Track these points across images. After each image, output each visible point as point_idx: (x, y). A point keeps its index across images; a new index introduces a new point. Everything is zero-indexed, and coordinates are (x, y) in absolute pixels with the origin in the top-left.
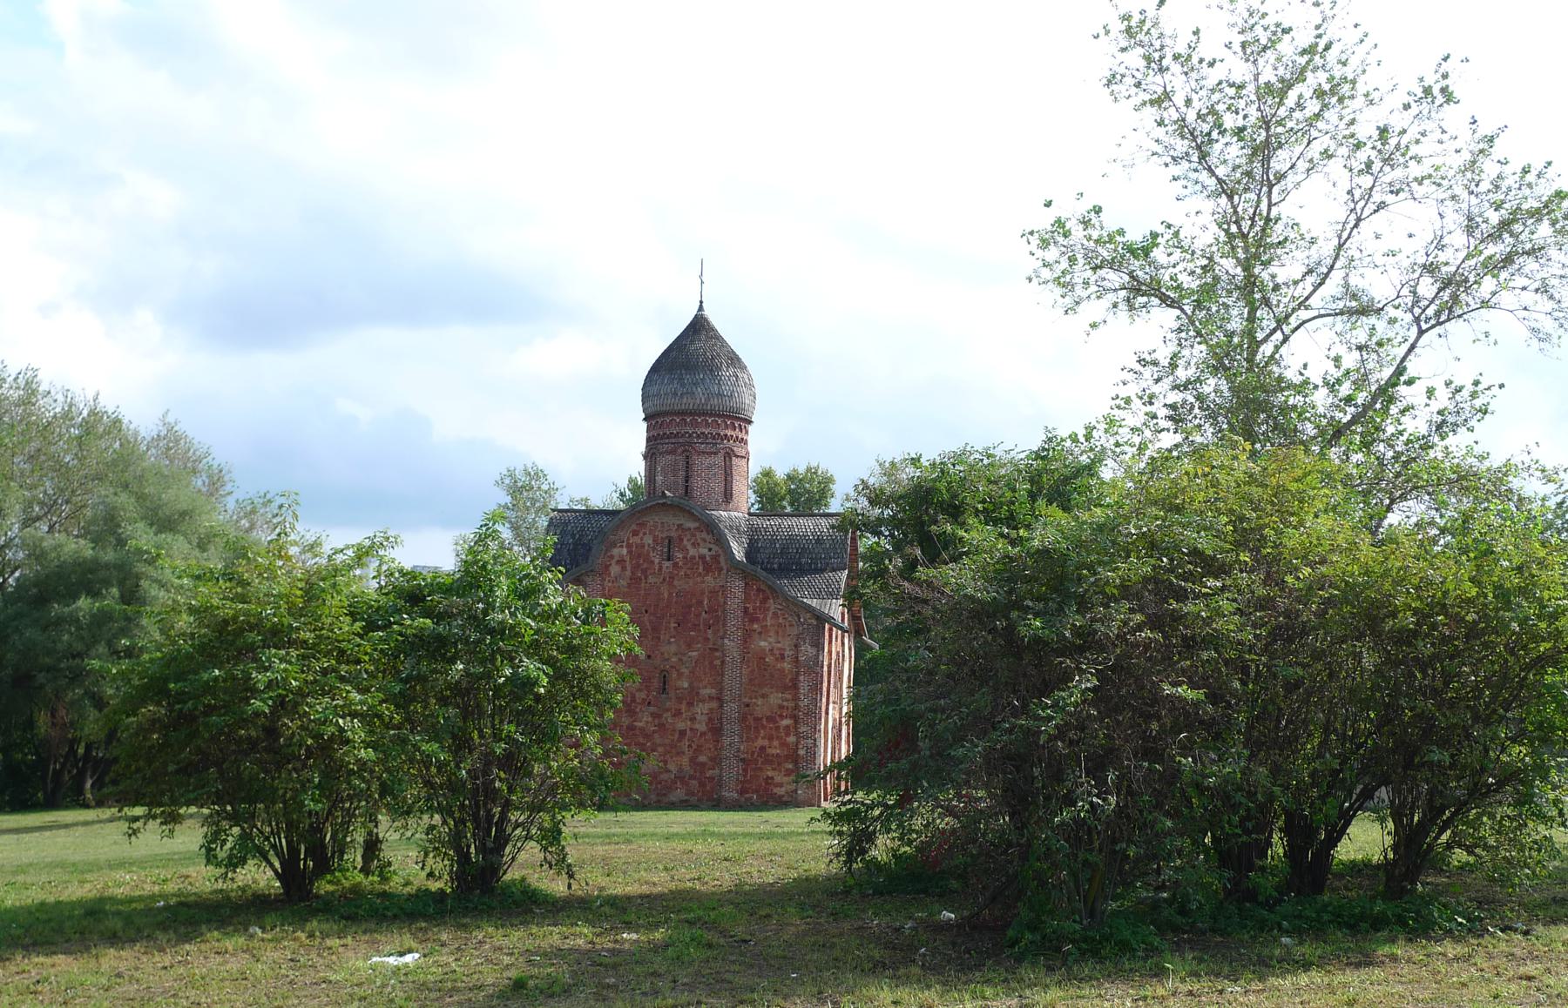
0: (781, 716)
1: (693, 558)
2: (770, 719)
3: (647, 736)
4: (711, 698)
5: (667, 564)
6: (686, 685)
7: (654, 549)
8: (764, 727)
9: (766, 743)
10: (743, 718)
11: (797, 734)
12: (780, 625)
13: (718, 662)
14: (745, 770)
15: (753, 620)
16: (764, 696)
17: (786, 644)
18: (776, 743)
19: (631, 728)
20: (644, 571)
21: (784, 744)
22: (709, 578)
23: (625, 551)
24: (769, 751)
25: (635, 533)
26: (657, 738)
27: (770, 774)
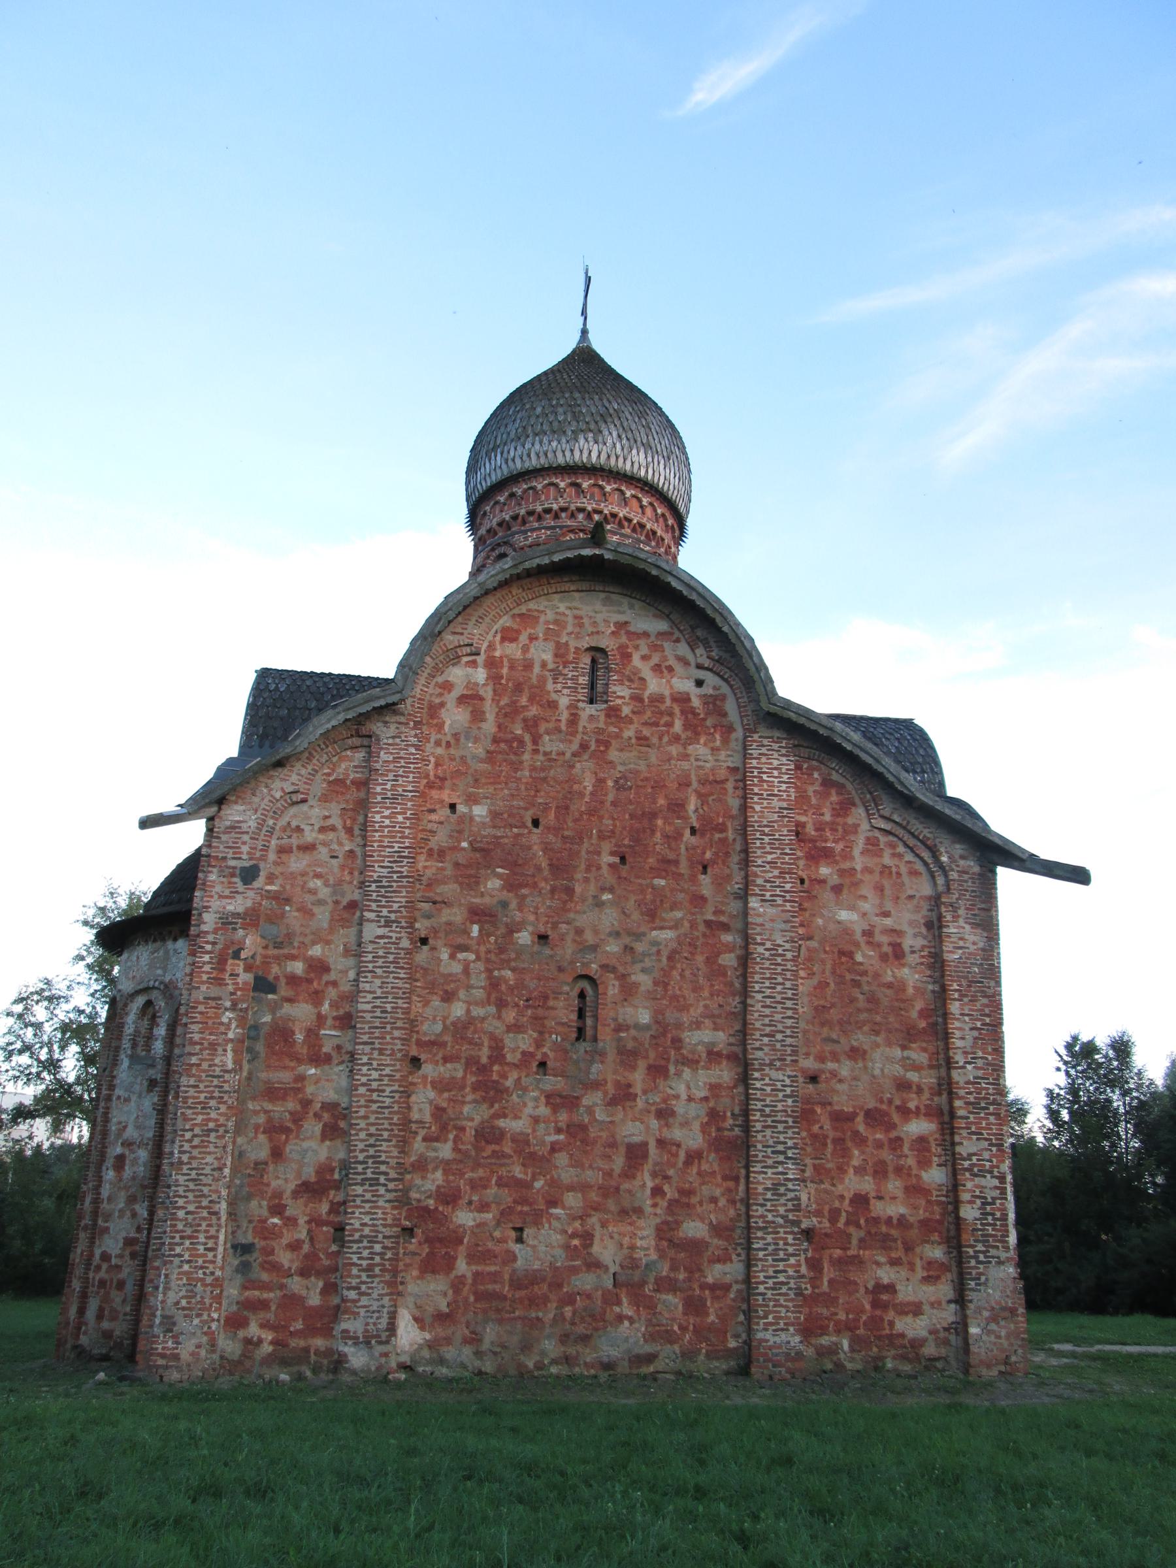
0: (905, 1112)
1: (658, 699)
2: (874, 1117)
3: (536, 1161)
4: (714, 1056)
5: (591, 710)
6: (645, 1017)
7: (556, 674)
8: (861, 1141)
9: (867, 1185)
10: (805, 1116)
11: (952, 1162)
12: (885, 870)
13: (729, 960)
14: (815, 1265)
15: (818, 854)
16: (856, 1053)
17: (907, 922)
18: (894, 1185)
19: (488, 1135)
20: (531, 725)
21: (915, 1190)
22: (699, 749)
23: (480, 675)
24: (879, 1209)
25: (509, 636)
26: (564, 1168)
27: (886, 1275)
